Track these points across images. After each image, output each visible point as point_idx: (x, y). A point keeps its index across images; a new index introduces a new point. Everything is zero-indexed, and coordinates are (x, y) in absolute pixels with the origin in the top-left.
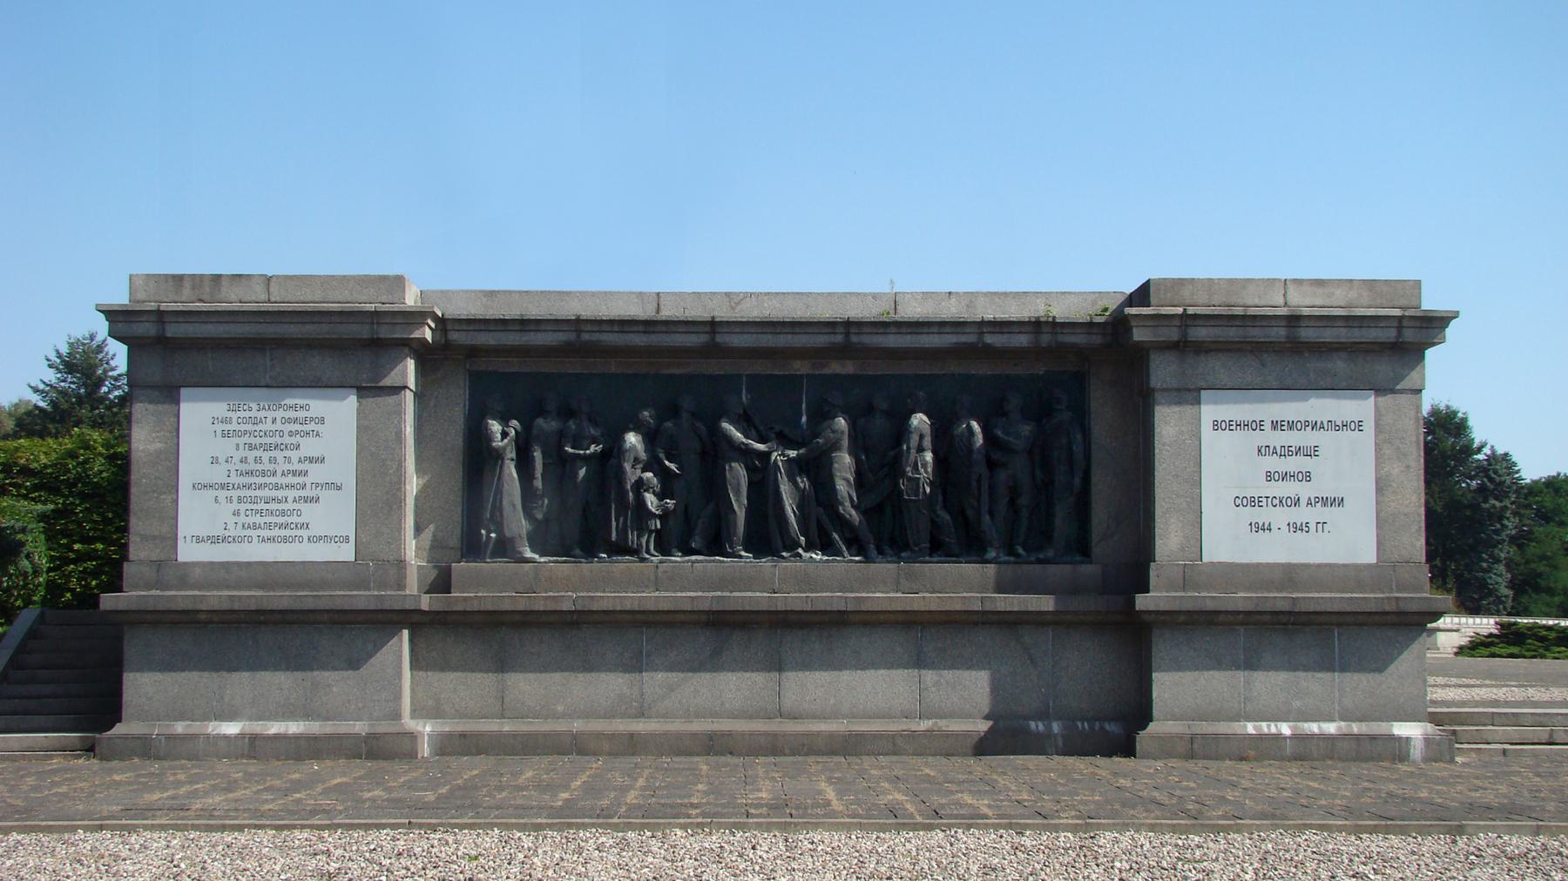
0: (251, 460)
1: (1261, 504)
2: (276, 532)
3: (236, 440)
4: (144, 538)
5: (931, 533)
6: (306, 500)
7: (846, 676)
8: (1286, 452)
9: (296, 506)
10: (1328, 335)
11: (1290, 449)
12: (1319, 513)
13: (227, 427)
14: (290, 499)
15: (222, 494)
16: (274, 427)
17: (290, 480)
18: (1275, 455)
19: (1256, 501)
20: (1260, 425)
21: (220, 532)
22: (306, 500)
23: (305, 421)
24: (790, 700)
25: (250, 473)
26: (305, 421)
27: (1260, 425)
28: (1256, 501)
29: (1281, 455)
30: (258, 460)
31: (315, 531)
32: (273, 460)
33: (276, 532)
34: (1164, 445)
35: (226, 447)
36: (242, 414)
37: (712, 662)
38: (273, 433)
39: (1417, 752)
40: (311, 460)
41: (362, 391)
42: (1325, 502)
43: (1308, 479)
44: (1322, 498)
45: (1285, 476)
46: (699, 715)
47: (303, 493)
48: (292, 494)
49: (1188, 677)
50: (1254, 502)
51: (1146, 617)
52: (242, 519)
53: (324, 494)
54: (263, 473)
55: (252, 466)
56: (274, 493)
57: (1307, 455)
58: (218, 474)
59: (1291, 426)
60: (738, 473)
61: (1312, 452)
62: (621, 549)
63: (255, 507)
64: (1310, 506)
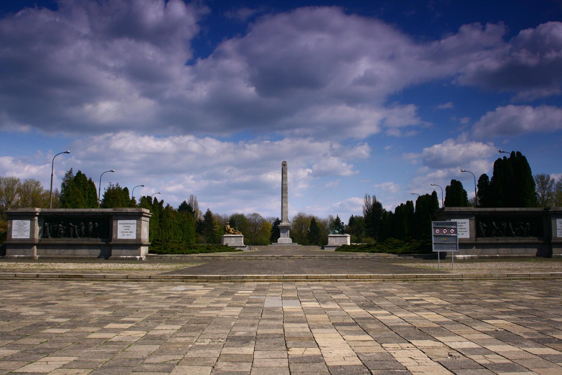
7: (82, 250)
8: (127, 227)
10: (130, 214)
20: (124, 224)
24: (76, 253)
27: (124, 224)
31: (26, 235)
35: (17, 226)
37: (68, 249)
39: (138, 259)
41: (31, 220)
45: (127, 229)
46: (66, 255)
49: (116, 250)
50: (123, 232)
58: (16, 229)
59: (127, 224)
60: (72, 229)
61: (130, 227)
62: (59, 237)
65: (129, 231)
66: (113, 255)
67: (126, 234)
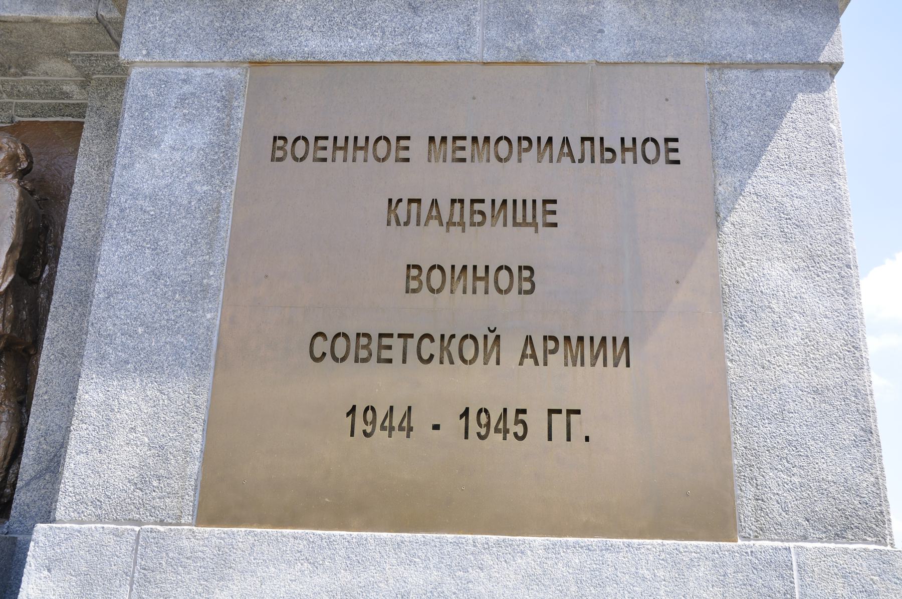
1: (385, 354)
11: (477, 206)
18: (434, 223)
19: (374, 346)
28: (374, 346)
29: (450, 223)
43: (527, 286)
44: (567, 339)
57: (525, 224)
64: (529, 362)
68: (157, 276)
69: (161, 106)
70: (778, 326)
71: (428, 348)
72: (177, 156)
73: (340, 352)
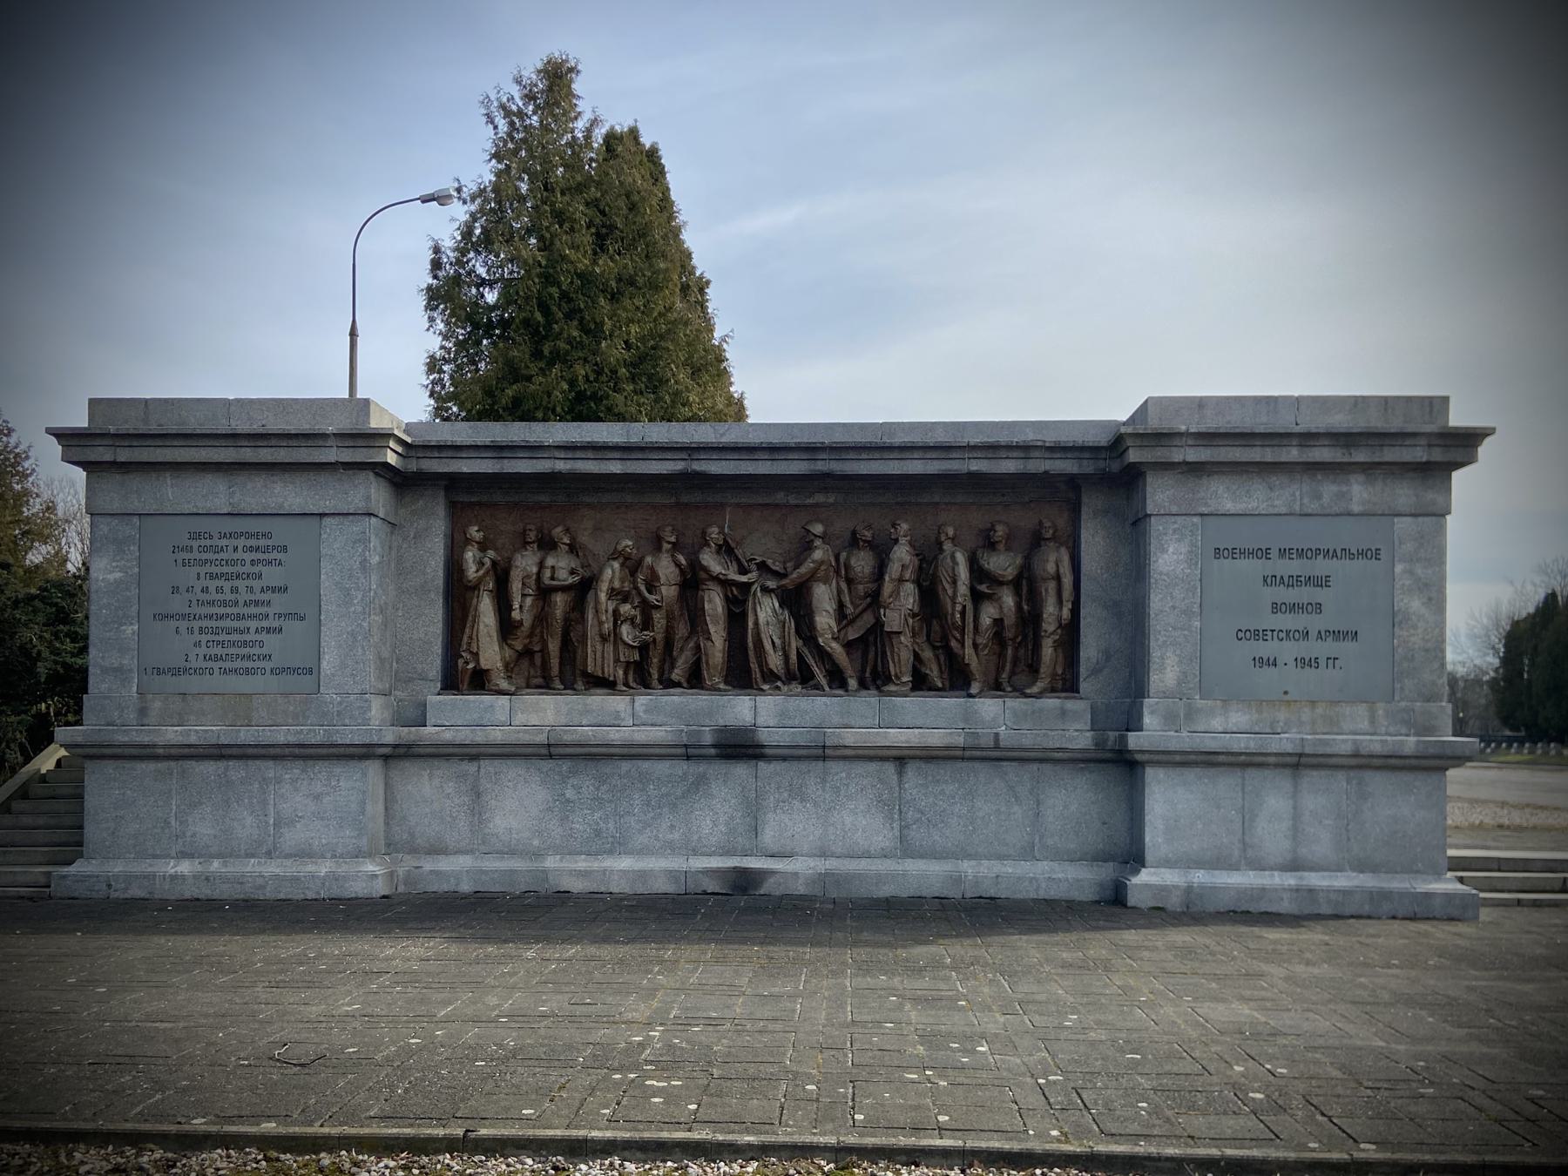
0: (212, 589)
2: (238, 664)
3: (197, 569)
4: (105, 671)
5: (914, 666)
6: (268, 630)
8: (1294, 581)
9: (259, 637)
12: (1327, 648)
13: (186, 556)
14: (252, 630)
15: (183, 625)
16: (235, 556)
17: (253, 610)
21: (183, 664)
22: (268, 630)
23: (266, 550)
25: (211, 603)
26: (266, 550)
30: (219, 590)
32: (234, 590)
33: (238, 664)
34: (1161, 573)
36: (203, 543)
38: (233, 562)
40: (273, 590)
42: (1337, 635)
45: (1294, 608)
47: (265, 624)
48: (253, 624)
50: (1258, 635)
51: (1138, 757)
52: (203, 650)
53: (288, 625)
54: (225, 604)
55: (214, 596)
56: (236, 624)
57: (1318, 586)
59: (1301, 553)
61: (1322, 582)
63: (216, 638)
64: (1319, 640)
65: (1314, 623)
66: (1168, 863)
67: (1288, 651)
68: (1174, 607)
69: (1165, 534)
70: (1415, 627)
71: (1281, 635)
72: (1175, 557)
73: (1248, 637)
